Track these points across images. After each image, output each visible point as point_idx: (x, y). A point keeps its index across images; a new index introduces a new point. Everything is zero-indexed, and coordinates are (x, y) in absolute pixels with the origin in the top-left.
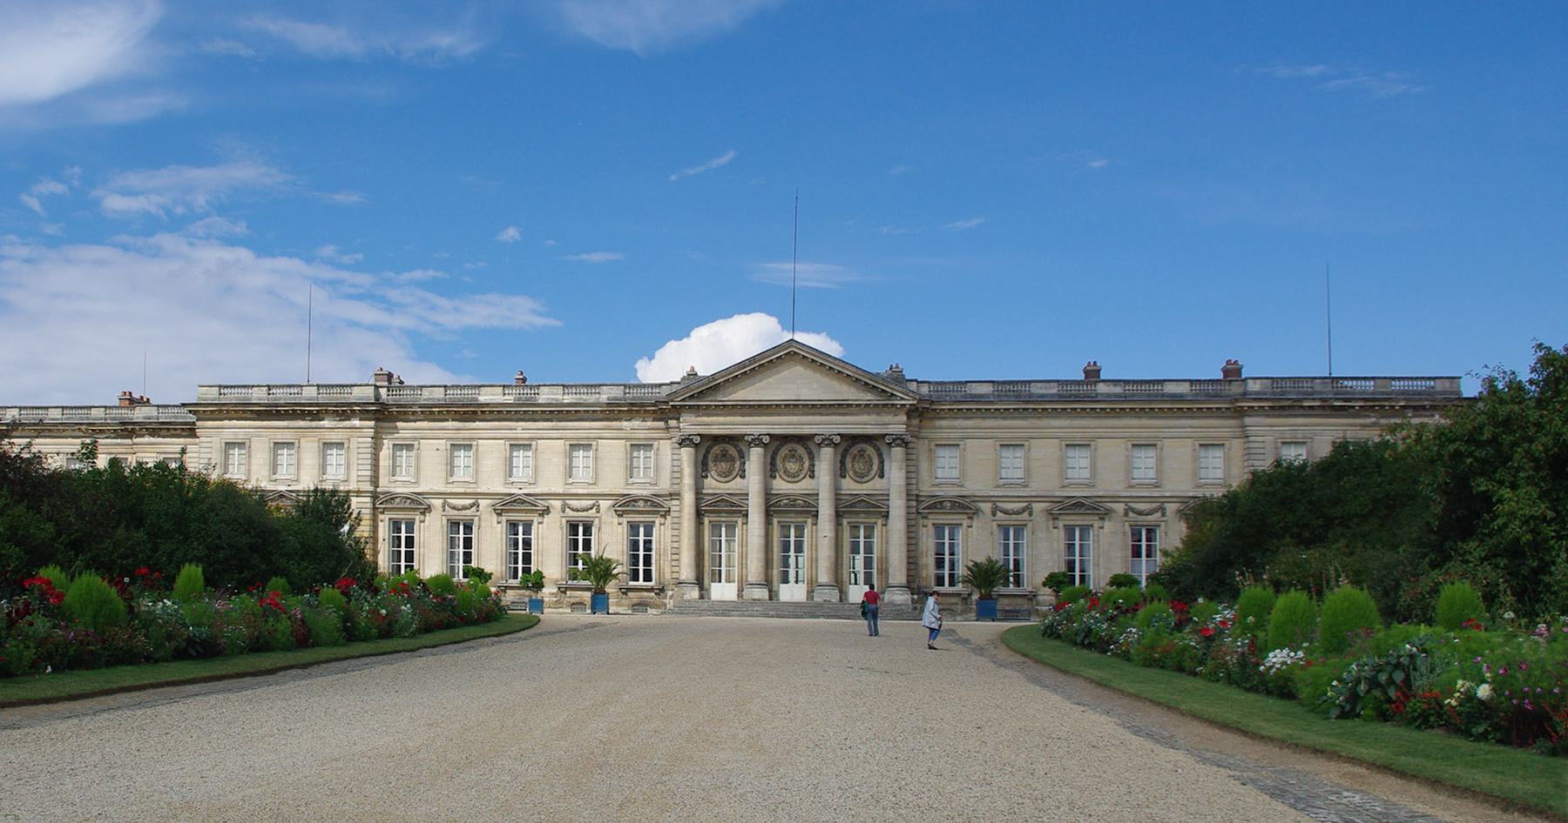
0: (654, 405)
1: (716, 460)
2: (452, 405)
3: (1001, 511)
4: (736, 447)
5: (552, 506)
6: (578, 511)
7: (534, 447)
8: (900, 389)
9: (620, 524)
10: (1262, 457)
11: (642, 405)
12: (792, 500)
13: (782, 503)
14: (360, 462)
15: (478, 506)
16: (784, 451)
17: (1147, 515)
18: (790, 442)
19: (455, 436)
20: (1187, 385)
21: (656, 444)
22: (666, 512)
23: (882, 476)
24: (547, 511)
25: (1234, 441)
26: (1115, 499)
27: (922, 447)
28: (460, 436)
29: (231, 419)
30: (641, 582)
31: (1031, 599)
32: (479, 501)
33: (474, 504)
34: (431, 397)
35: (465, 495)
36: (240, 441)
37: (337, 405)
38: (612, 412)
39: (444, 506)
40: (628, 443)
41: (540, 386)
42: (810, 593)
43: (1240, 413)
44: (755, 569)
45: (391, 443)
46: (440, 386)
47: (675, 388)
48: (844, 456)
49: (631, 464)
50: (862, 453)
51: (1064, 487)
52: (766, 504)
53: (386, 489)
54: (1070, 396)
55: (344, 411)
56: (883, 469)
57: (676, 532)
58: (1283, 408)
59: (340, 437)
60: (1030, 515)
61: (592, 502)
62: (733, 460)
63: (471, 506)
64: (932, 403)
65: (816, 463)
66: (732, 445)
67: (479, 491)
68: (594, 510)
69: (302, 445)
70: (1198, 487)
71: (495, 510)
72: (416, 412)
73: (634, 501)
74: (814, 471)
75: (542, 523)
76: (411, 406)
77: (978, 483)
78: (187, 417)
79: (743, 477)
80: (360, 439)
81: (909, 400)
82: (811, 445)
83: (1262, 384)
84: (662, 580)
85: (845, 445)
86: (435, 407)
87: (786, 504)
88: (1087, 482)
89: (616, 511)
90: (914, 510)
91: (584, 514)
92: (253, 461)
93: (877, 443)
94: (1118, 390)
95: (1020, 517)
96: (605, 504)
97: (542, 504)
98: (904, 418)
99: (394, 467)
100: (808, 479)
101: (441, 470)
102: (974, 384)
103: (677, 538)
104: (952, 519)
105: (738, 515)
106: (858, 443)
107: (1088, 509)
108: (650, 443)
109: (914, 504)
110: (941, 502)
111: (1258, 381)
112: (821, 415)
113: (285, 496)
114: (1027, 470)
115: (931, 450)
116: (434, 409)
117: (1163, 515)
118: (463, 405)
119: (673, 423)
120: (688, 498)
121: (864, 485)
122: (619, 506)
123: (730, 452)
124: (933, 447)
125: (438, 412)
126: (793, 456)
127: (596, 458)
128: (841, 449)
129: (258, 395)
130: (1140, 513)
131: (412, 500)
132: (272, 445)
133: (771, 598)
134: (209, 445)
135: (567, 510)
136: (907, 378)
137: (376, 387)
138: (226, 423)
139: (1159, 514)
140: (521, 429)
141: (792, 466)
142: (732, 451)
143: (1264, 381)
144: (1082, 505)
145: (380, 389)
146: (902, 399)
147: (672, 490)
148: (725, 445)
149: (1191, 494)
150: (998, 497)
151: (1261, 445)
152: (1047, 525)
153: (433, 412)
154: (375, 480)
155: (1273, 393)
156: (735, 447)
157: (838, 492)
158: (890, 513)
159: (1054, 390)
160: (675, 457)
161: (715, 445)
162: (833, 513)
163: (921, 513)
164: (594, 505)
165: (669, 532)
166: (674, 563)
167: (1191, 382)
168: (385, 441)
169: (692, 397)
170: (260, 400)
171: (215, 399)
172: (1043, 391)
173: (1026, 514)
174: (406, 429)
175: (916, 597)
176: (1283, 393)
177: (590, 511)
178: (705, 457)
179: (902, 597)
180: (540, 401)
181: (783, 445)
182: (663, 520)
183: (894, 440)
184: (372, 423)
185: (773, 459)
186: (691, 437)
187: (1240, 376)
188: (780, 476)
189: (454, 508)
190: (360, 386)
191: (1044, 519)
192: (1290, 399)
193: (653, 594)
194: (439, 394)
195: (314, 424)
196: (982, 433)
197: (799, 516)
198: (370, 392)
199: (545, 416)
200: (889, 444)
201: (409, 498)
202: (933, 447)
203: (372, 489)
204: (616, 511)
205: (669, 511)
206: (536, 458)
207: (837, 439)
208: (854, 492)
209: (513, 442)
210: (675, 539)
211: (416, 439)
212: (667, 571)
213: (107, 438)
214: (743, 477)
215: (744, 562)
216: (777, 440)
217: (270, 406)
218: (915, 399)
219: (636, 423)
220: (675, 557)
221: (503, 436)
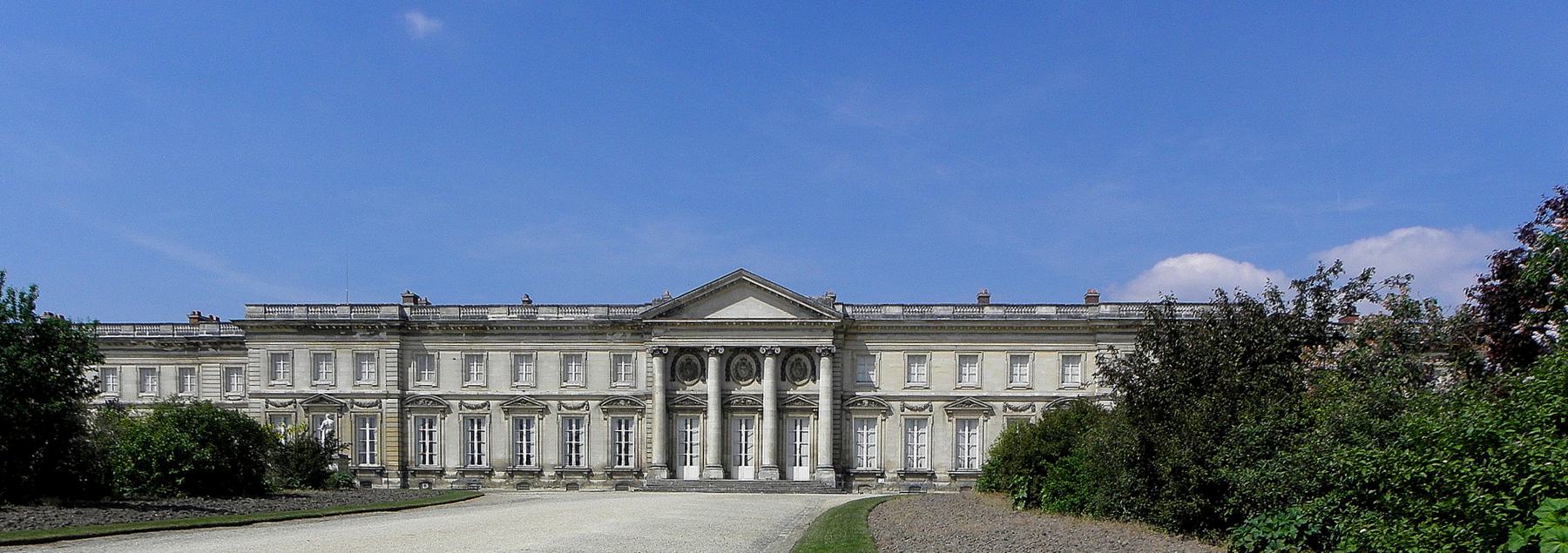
6: (570, 409)
7: (534, 357)
9: (605, 419)
12: (744, 400)
15: (489, 406)
16: (736, 360)
17: (1021, 411)
19: (469, 348)
27: (847, 357)
30: (623, 466)
33: (486, 404)
35: (477, 397)
39: (460, 406)
41: (538, 306)
42: (756, 473)
44: (712, 456)
46: (455, 306)
47: (649, 307)
48: (784, 364)
54: (963, 317)
55: (372, 328)
57: (649, 426)
60: (931, 411)
67: (489, 393)
78: (235, 332)
81: (832, 319)
85: (785, 354)
89: (602, 409)
90: (839, 407)
91: (576, 412)
95: (922, 413)
107: (975, 406)
109: (839, 402)
113: (325, 399)
115: (853, 359)
117: (1034, 411)
120: (658, 397)
126: (744, 364)
128: (781, 359)
129: (298, 314)
130: (1016, 410)
131: (434, 401)
133: (725, 477)
137: (401, 307)
142: (696, 360)
149: (1054, 395)
152: (944, 420)
153: (451, 329)
154: (402, 384)
160: (649, 365)
164: (584, 404)
165: (645, 426)
169: (661, 316)
172: (942, 313)
175: (840, 476)
179: (828, 476)
180: (539, 319)
183: (823, 351)
185: (728, 367)
189: (468, 407)
190: (387, 305)
194: (454, 312)
198: (395, 311)
200: (820, 354)
203: (399, 392)
204: (602, 409)
211: (435, 351)
212: (644, 457)
213: (175, 350)
216: (730, 350)
220: (649, 446)
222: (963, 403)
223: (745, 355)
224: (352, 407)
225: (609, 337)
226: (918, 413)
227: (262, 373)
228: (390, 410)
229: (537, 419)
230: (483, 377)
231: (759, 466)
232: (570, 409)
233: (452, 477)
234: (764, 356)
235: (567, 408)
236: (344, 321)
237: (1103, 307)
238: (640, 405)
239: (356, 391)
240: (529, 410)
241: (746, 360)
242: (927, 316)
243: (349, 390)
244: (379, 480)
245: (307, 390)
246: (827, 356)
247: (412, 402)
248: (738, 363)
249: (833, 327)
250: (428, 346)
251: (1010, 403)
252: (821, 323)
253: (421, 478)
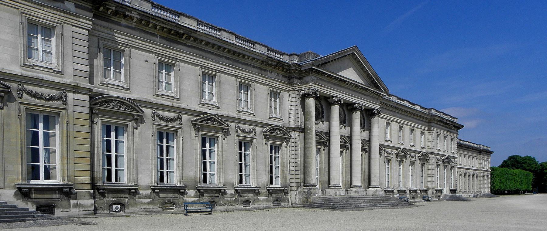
108: (279, 91)
146: (383, 92)
224: (21, 97)
225: (269, 74)
226: (389, 155)
228: (79, 109)
233: (146, 197)
240: (216, 129)
244: (64, 202)
247: (101, 103)
250: (120, 38)
253: (111, 198)
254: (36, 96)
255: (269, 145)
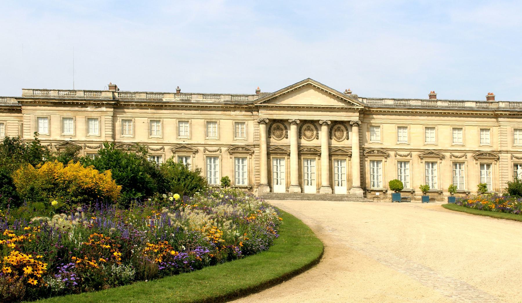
0: (246, 105)
1: (275, 129)
2: (151, 102)
3: (398, 155)
4: (283, 124)
5: (199, 150)
6: (211, 152)
7: (190, 122)
8: (357, 101)
9: (231, 158)
10: (506, 135)
11: (241, 105)
13: (305, 150)
14: (107, 127)
16: (305, 127)
17: (460, 158)
18: (308, 123)
20: (475, 103)
21: (246, 122)
22: (252, 153)
23: (348, 139)
24: (197, 152)
25: (494, 127)
26: (446, 151)
27: (365, 126)
28: (155, 116)
29: (40, 106)
31: (412, 193)
32: (165, 147)
34: (140, 98)
36: (45, 116)
37: (95, 101)
38: (227, 107)
40: (234, 122)
43: (496, 116)
45: (121, 119)
49: (236, 131)
50: (339, 128)
51: (425, 145)
52: (298, 150)
53: (119, 141)
54: (426, 106)
55: (98, 104)
56: (348, 136)
57: (257, 162)
58: (514, 114)
59: (96, 116)
60: (411, 157)
61: (218, 148)
62: (282, 130)
63: (161, 149)
64: (369, 108)
65: (319, 132)
66: (282, 124)
67: (164, 142)
68: (219, 152)
69: (77, 119)
70: (480, 146)
71: (172, 151)
72: (133, 105)
73: (237, 148)
74: (318, 136)
75: (195, 157)
76: (131, 102)
77: (389, 143)
79: (287, 138)
80: (106, 117)
82: (316, 124)
83: (505, 104)
84: (251, 184)
86: (143, 103)
87: (306, 150)
88: (433, 143)
90: (362, 154)
92: (52, 126)
93: (345, 124)
94: (446, 104)
96: (224, 149)
97: (194, 149)
98: (358, 114)
99: (123, 130)
100: (315, 139)
101: (59, 132)
102: (386, 100)
103: (259, 165)
104: (378, 158)
105: (285, 155)
106: (337, 124)
110: (373, 151)
111: (504, 103)
112: (322, 111)
113: (69, 144)
114: (410, 138)
115: (368, 128)
116: (142, 104)
117: (466, 158)
118: (156, 103)
119: (255, 113)
120: (264, 147)
121: (340, 142)
122: (231, 150)
123: (281, 127)
124: (369, 127)
125: (144, 105)
126: (309, 129)
127: (219, 128)
129: (52, 94)
130: (457, 157)
132: (62, 119)
133: (302, 192)
134: (29, 118)
135: (206, 151)
136: (359, 96)
137: (113, 92)
138: (38, 107)
139: (464, 157)
140: (184, 114)
141: (308, 133)
143: (506, 103)
144: (433, 153)
145: (115, 93)
147: (255, 143)
148: (279, 124)
149: (477, 150)
150: (397, 149)
151: (505, 130)
152: (418, 161)
153: (141, 105)
154: (114, 136)
155: (510, 108)
156: (283, 125)
157: (330, 145)
158: (352, 155)
159: (419, 103)
161: (274, 123)
162: (328, 155)
163: (365, 155)
164: (219, 150)
166: (257, 176)
167: (476, 102)
168: (118, 118)
170: (55, 97)
171: (31, 96)
173: (409, 157)
174: (129, 113)
176: (514, 108)
177: (217, 152)
178: (270, 129)
180: (192, 101)
181: (304, 124)
182: (250, 156)
183: (354, 123)
184: (112, 110)
186: (265, 120)
187: (494, 100)
188: (304, 138)
191: (417, 158)
192: (517, 111)
193: (247, 190)
194: (143, 96)
195: (83, 109)
196: (389, 121)
197: (312, 155)
199: (194, 108)
201: (131, 145)
202: (369, 127)
203: (112, 140)
205: (254, 152)
206: (191, 127)
207: (267, 121)
208: (336, 146)
209: (180, 120)
210: (257, 165)
214: (287, 138)
215: (289, 176)
217: (61, 100)
218: (363, 106)
219: (237, 113)
221: (148, 116)
222: (429, 153)
223: (309, 125)
226: (404, 158)
227: (31, 128)
229: (191, 157)
230: (160, 132)
231: (319, 187)
232: (211, 152)
234: (321, 125)
235: (209, 151)
236: (82, 100)
237: (501, 103)
238: (251, 151)
239: (88, 140)
241: (310, 127)
242: (407, 106)
243: (83, 139)
245: (59, 138)
246: (356, 126)
248: (305, 129)
249: (358, 110)
251: (514, 154)
252: (353, 108)
254: (90, 147)
255: (233, 158)
